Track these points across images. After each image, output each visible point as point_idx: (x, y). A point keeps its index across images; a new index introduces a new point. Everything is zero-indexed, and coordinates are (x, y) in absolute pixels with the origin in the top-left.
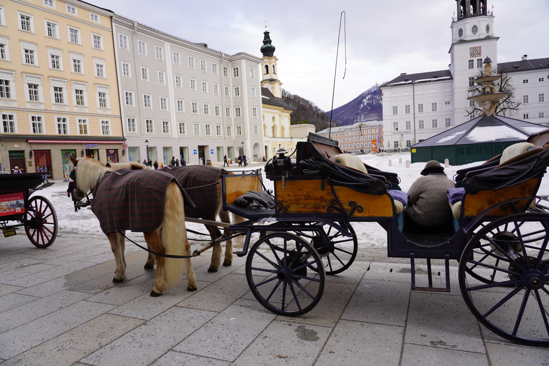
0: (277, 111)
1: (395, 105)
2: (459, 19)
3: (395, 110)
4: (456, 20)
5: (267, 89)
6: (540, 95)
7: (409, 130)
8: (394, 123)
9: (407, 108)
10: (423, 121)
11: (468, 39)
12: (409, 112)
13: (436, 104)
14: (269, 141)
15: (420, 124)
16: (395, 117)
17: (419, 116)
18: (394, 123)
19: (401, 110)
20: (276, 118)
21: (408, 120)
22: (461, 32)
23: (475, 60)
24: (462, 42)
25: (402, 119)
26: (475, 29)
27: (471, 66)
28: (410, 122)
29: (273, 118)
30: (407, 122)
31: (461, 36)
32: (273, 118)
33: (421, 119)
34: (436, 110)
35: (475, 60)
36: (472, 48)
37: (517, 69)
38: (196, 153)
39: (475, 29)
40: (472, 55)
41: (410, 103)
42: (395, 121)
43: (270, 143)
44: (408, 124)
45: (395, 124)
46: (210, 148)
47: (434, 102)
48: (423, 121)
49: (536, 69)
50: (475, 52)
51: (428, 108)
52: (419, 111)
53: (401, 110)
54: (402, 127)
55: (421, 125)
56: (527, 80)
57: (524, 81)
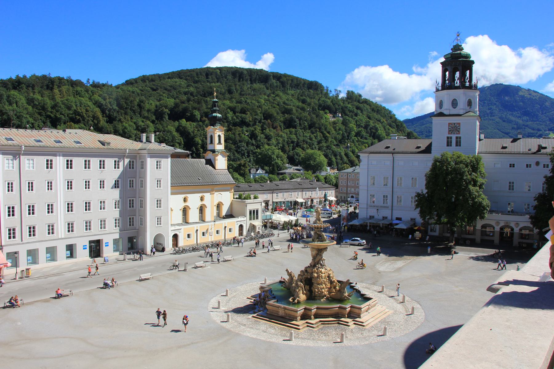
2: (444, 87)
4: (440, 88)
9: (386, 179)
11: (446, 112)
14: (180, 229)
20: (205, 198)
22: (440, 104)
23: (454, 137)
24: (441, 115)
26: (454, 104)
27: (449, 144)
29: (202, 199)
31: (441, 108)
32: (202, 199)
35: (454, 137)
36: (451, 124)
37: (504, 150)
38: (86, 248)
39: (454, 104)
40: (450, 131)
43: (182, 230)
46: (104, 242)
50: (454, 128)
56: (514, 165)
57: (510, 165)
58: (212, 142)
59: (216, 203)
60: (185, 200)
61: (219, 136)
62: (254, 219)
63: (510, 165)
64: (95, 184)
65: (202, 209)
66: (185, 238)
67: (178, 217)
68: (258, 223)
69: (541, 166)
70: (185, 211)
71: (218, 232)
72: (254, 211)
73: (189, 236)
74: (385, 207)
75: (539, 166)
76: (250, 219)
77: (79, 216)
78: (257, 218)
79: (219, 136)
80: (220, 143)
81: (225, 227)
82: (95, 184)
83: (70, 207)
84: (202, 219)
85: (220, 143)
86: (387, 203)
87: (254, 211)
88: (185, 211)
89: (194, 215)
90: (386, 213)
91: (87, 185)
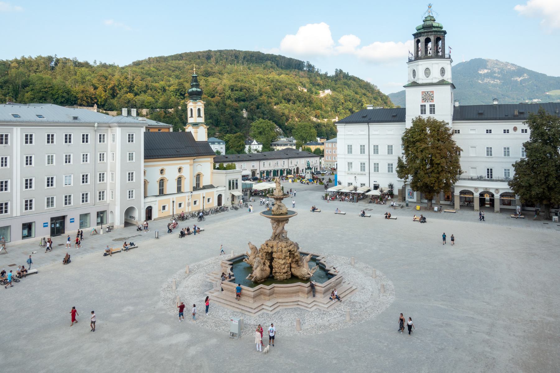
0: (188, 161)
1: (350, 144)
3: (350, 149)
5: (190, 132)
6: (505, 148)
7: (363, 172)
8: (348, 163)
10: (378, 164)
12: (364, 153)
13: (392, 146)
14: (156, 201)
15: (375, 167)
16: (350, 156)
17: (375, 159)
18: (348, 163)
19: (356, 149)
21: (363, 161)
25: (357, 158)
28: (364, 163)
29: (180, 170)
30: (361, 163)
32: (180, 170)
33: (376, 162)
34: (392, 153)
41: (365, 143)
42: (350, 161)
43: (157, 203)
44: (363, 166)
45: (350, 164)
47: (390, 144)
48: (378, 164)
49: (500, 119)
51: (383, 150)
52: (374, 153)
53: (356, 149)
54: (356, 168)
55: (376, 168)
56: (490, 130)
57: (487, 130)
58: (192, 116)
59: (195, 174)
60: (162, 171)
61: (199, 110)
62: (233, 188)
63: (487, 130)
64: (59, 159)
65: (179, 180)
66: (160, 210)
67: (154, 188)
68: (238, 193)
69: (519, 131)
70: (162, 182)
71: (195, 202)
72: (233, 181)
73: (164, 208)
74: (362, 174)
75: (517, 132)
76: (230, 189)
77: (39, 193)
78: (237, 188)
79: (199, 110)
80: (199, 116)
81: (204, 197)
82: (59, 159)
83: (28, 184)
84: (179, 190)
85: (199, 116)
86: (364, 170)
87: (233, 181)
88: (162, 182)
89: (171, 186)
90: (364, 179)
91: (50, 160)
